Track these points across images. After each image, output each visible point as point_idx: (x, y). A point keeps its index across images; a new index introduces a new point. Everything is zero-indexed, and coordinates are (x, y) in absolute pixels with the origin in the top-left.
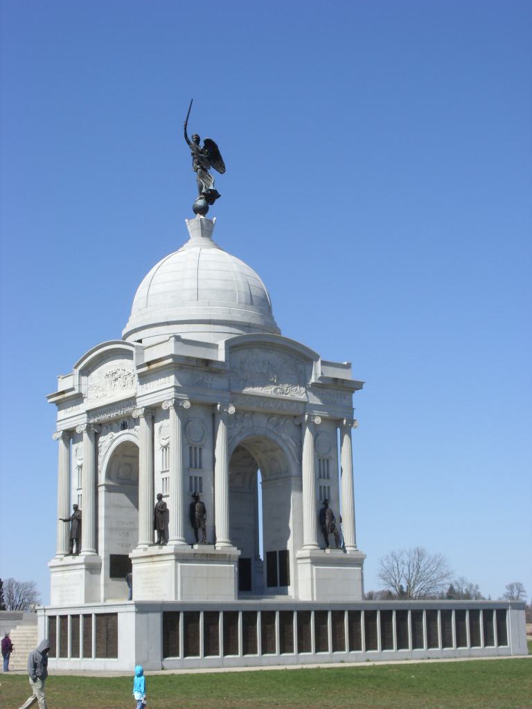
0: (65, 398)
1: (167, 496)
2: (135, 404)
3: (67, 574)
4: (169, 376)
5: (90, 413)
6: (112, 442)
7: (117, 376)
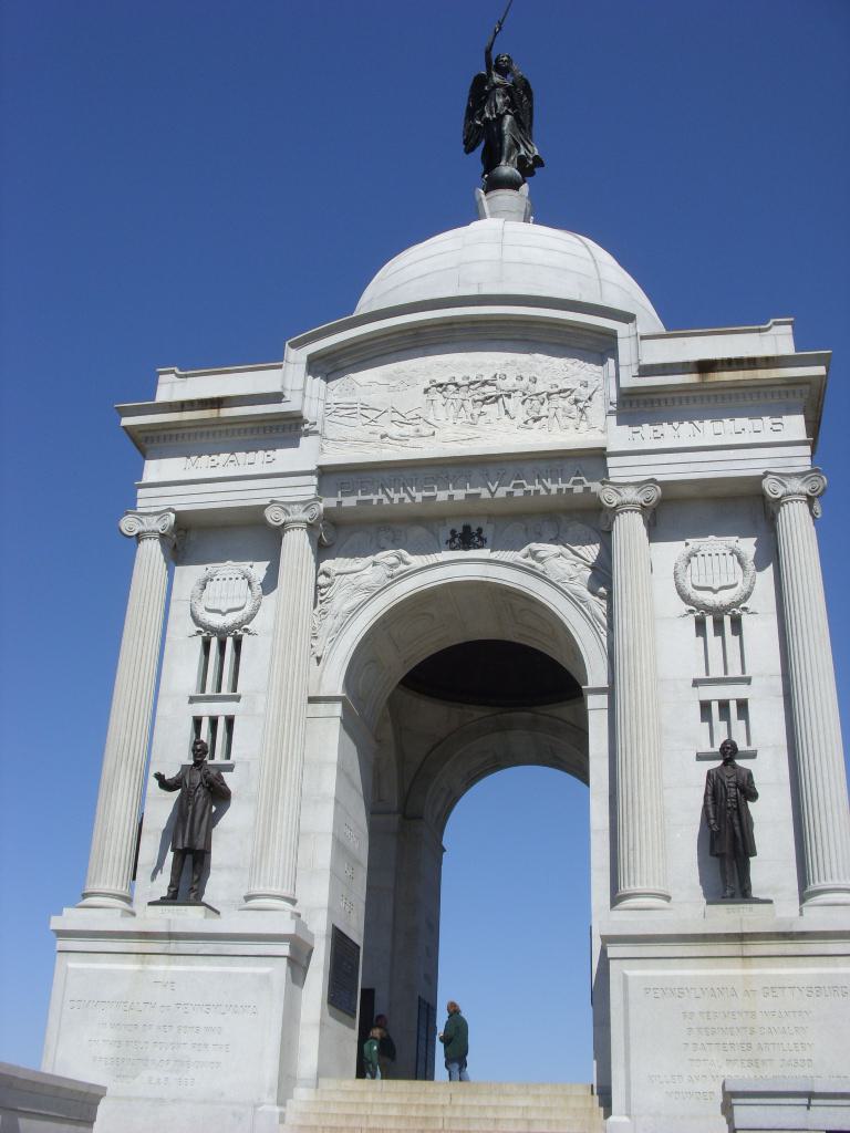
0: (220, 421)
1: (752, 755)
2: (602, 474)
3: (161, 967)
4: (776, 412)
5: (329, 476)
6: (396, 579)
7: (489, 390)
